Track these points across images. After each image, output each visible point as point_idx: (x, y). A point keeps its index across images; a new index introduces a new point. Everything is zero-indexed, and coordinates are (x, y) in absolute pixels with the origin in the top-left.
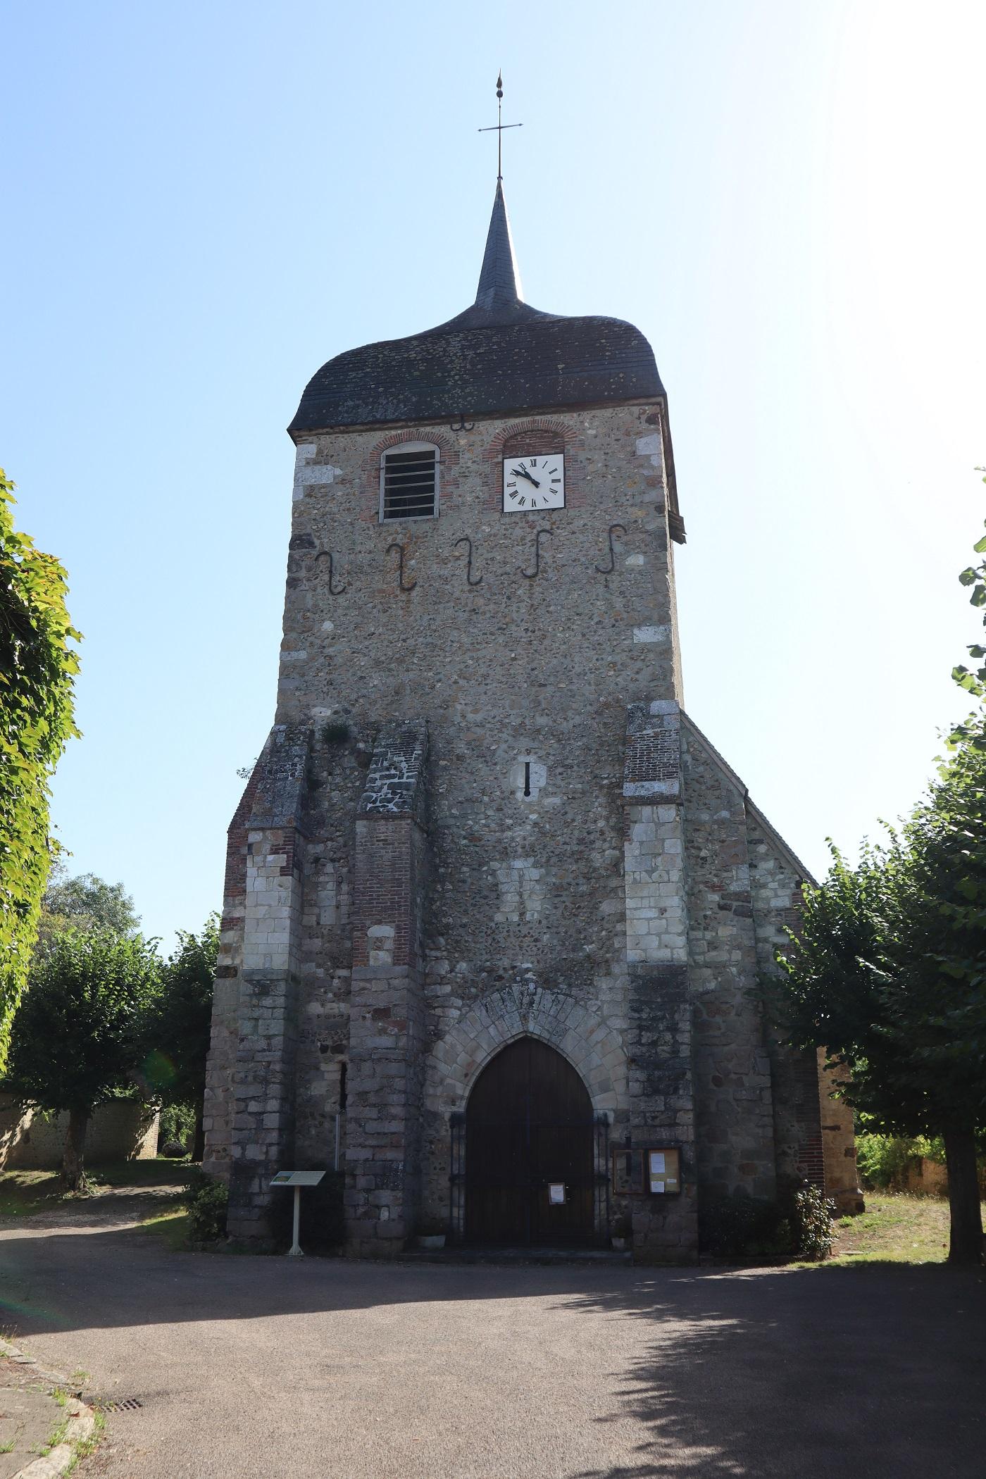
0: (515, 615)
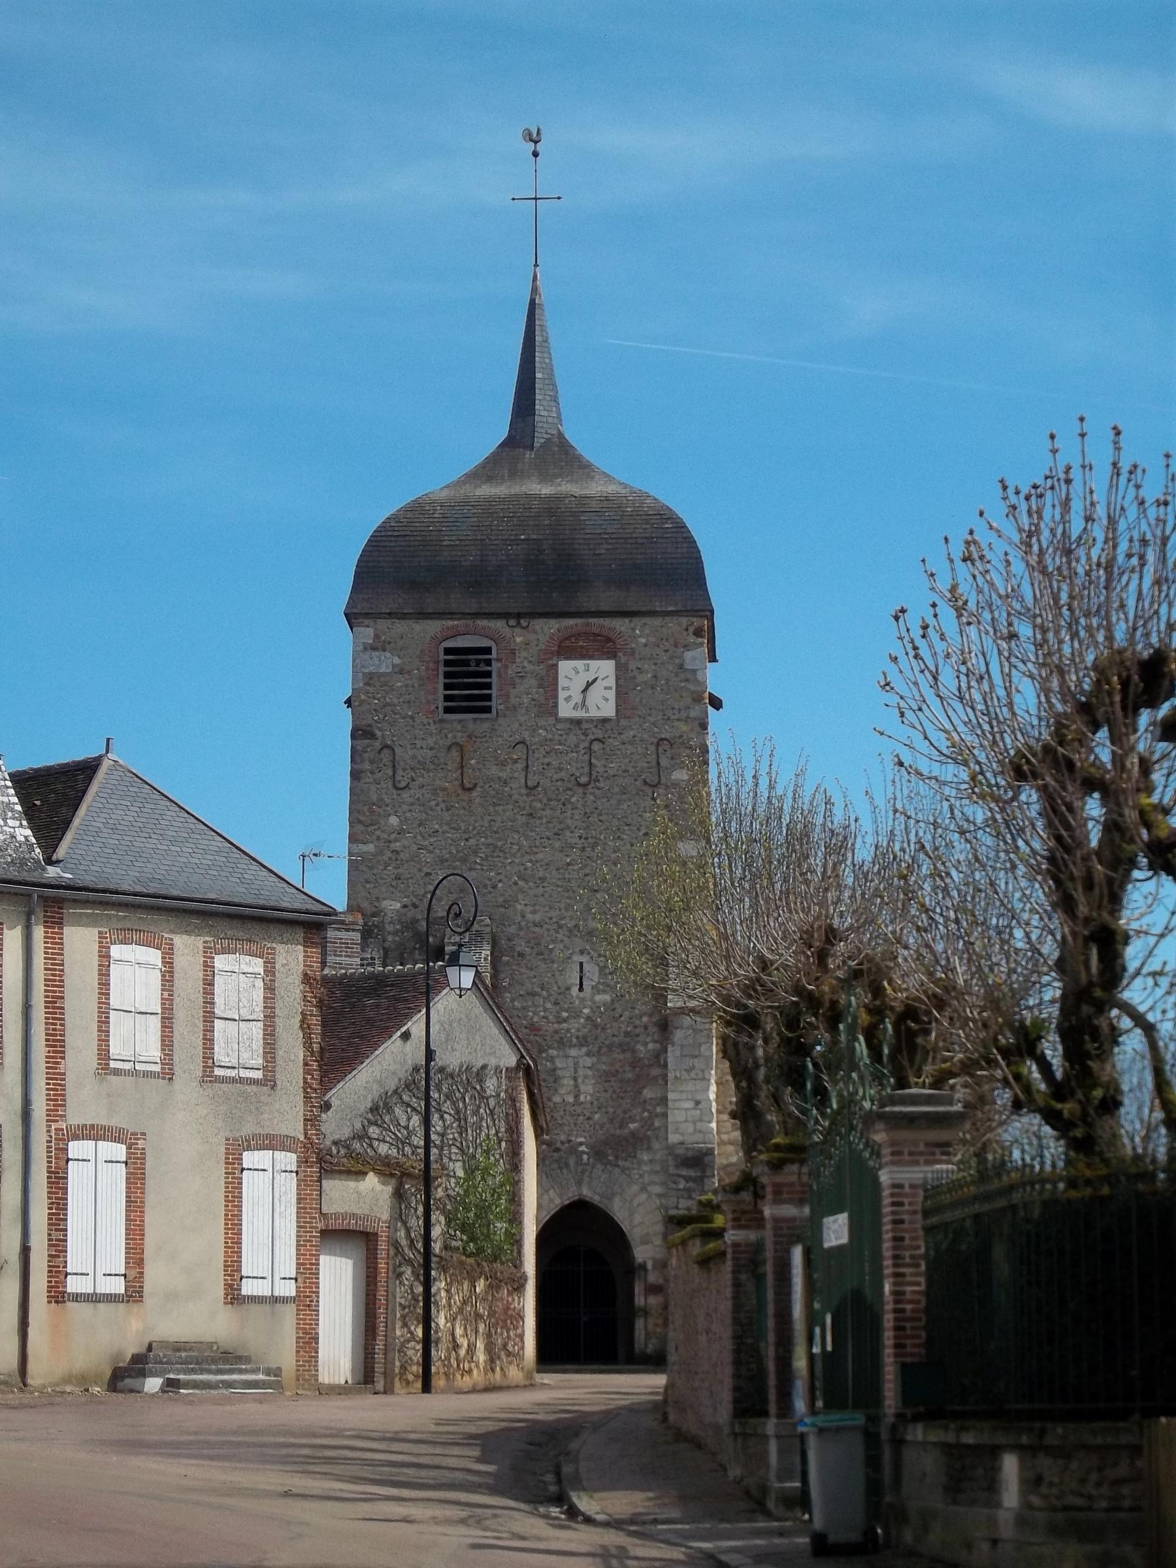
0: (569, 822)
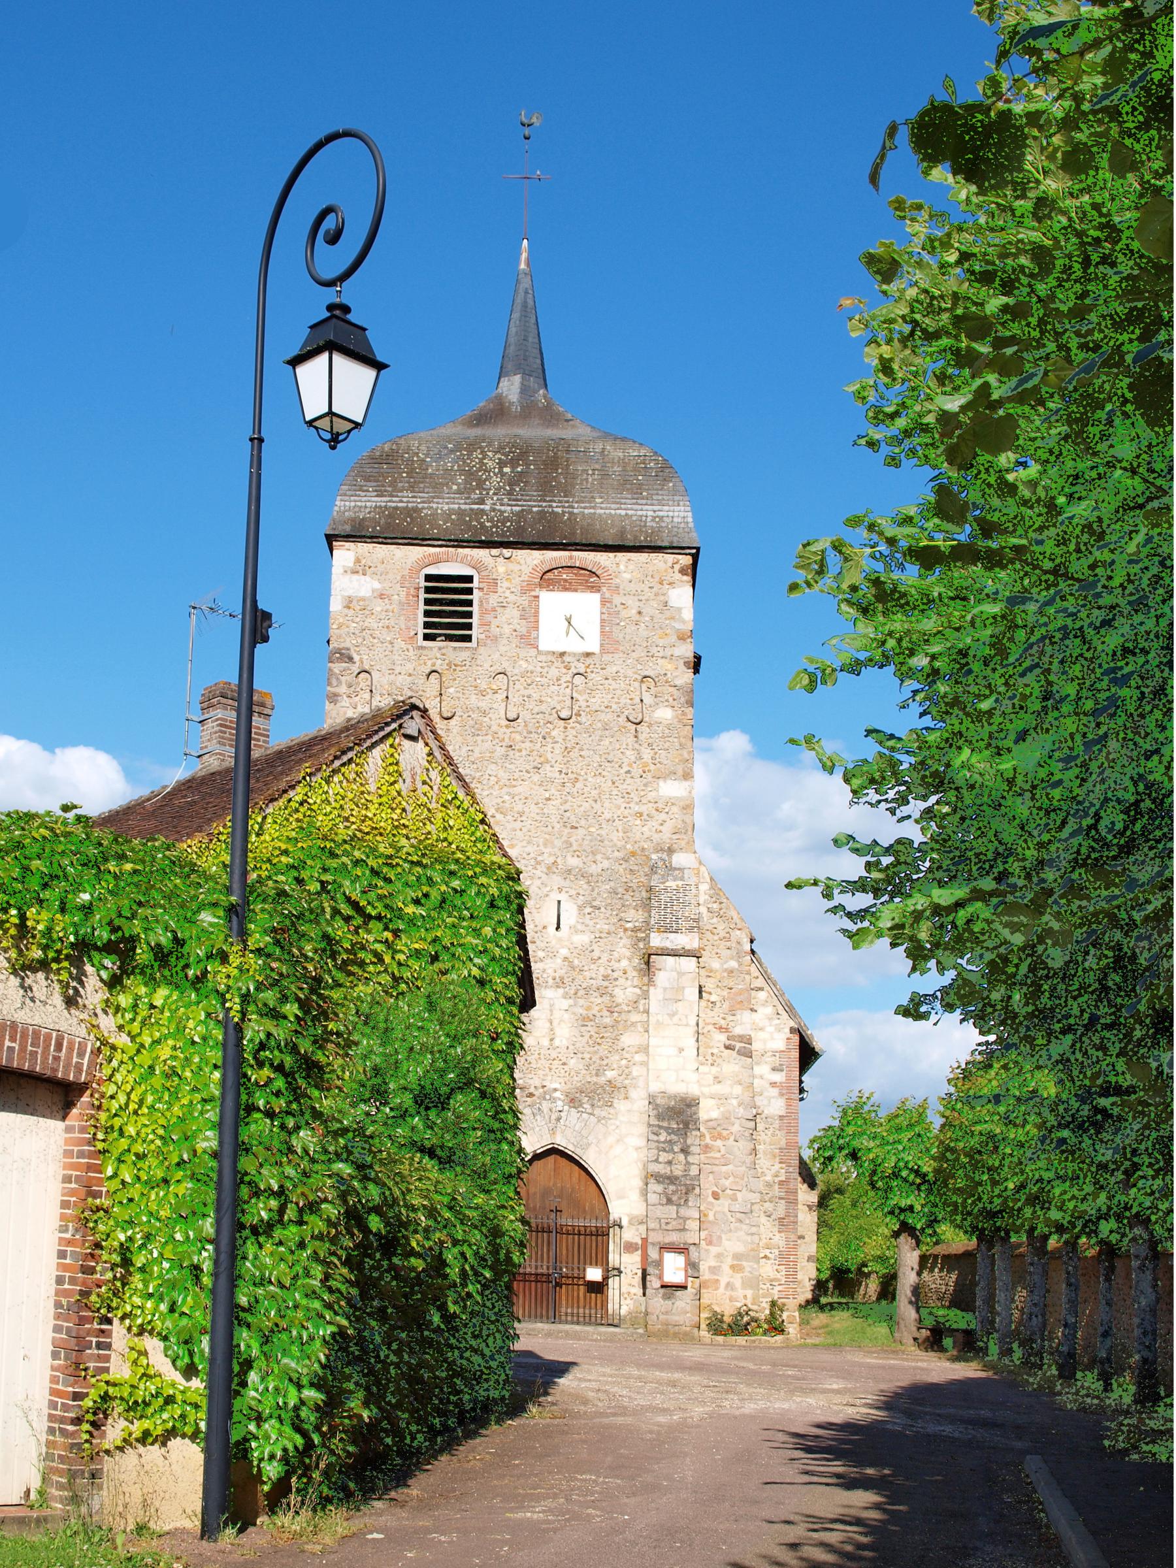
0: (549, 756)
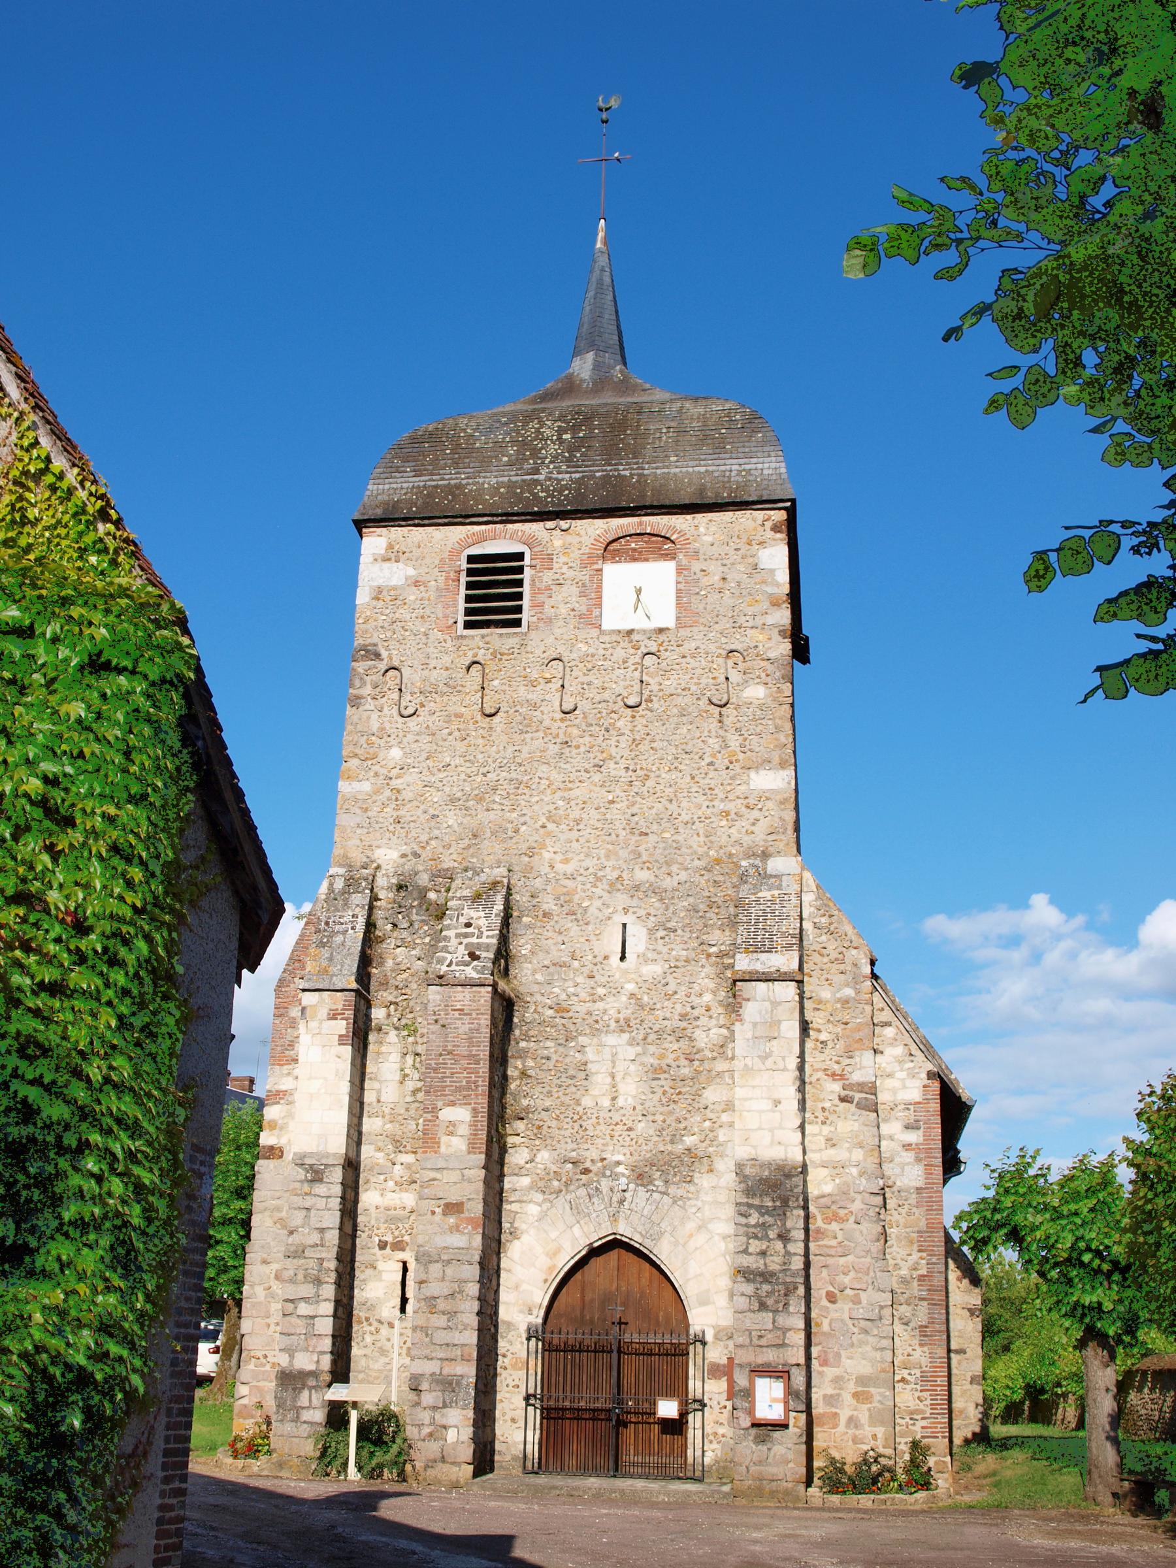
0: (613, 751)
